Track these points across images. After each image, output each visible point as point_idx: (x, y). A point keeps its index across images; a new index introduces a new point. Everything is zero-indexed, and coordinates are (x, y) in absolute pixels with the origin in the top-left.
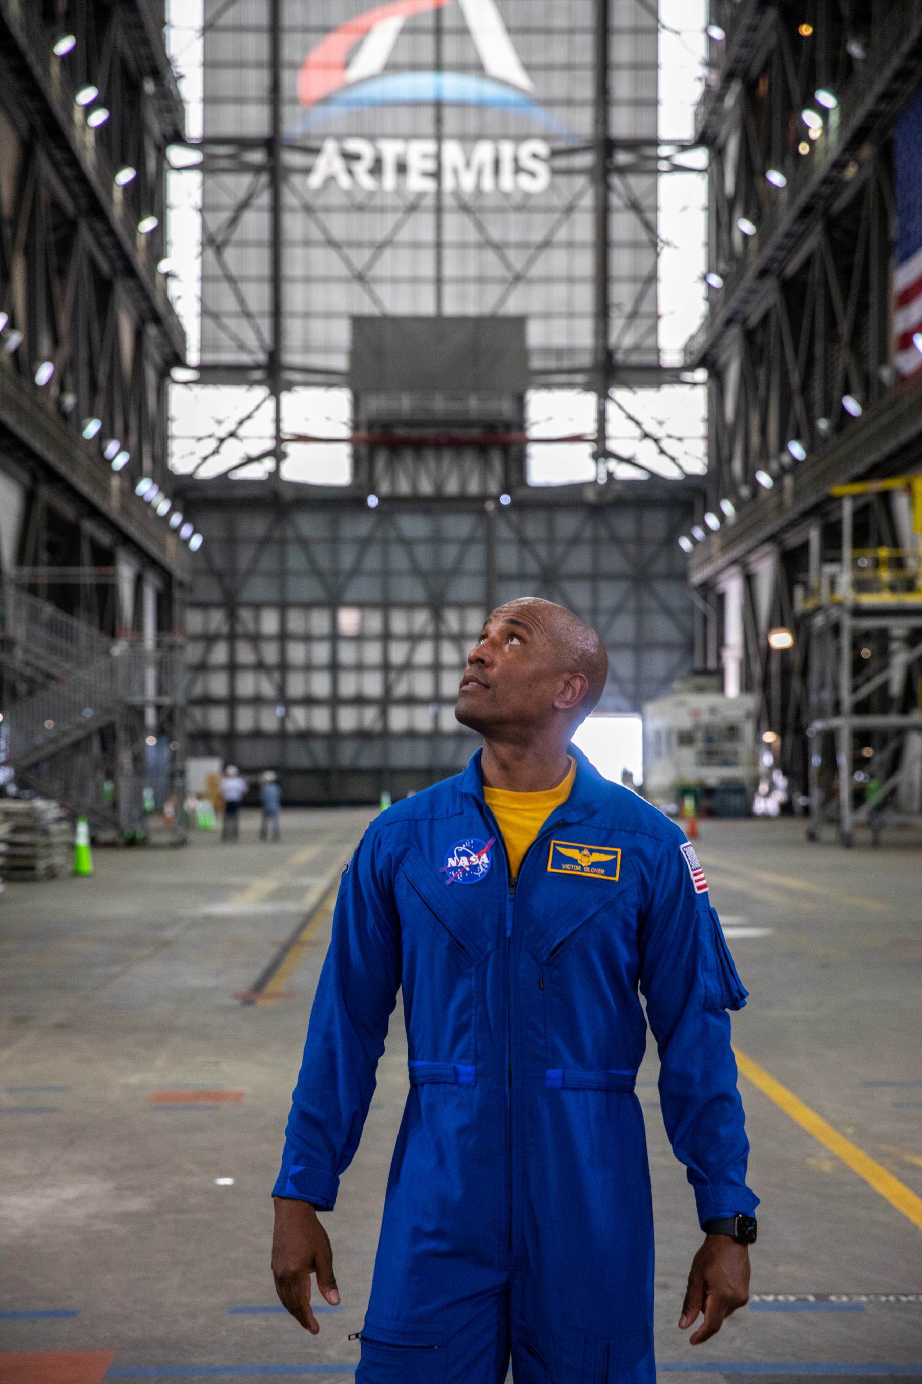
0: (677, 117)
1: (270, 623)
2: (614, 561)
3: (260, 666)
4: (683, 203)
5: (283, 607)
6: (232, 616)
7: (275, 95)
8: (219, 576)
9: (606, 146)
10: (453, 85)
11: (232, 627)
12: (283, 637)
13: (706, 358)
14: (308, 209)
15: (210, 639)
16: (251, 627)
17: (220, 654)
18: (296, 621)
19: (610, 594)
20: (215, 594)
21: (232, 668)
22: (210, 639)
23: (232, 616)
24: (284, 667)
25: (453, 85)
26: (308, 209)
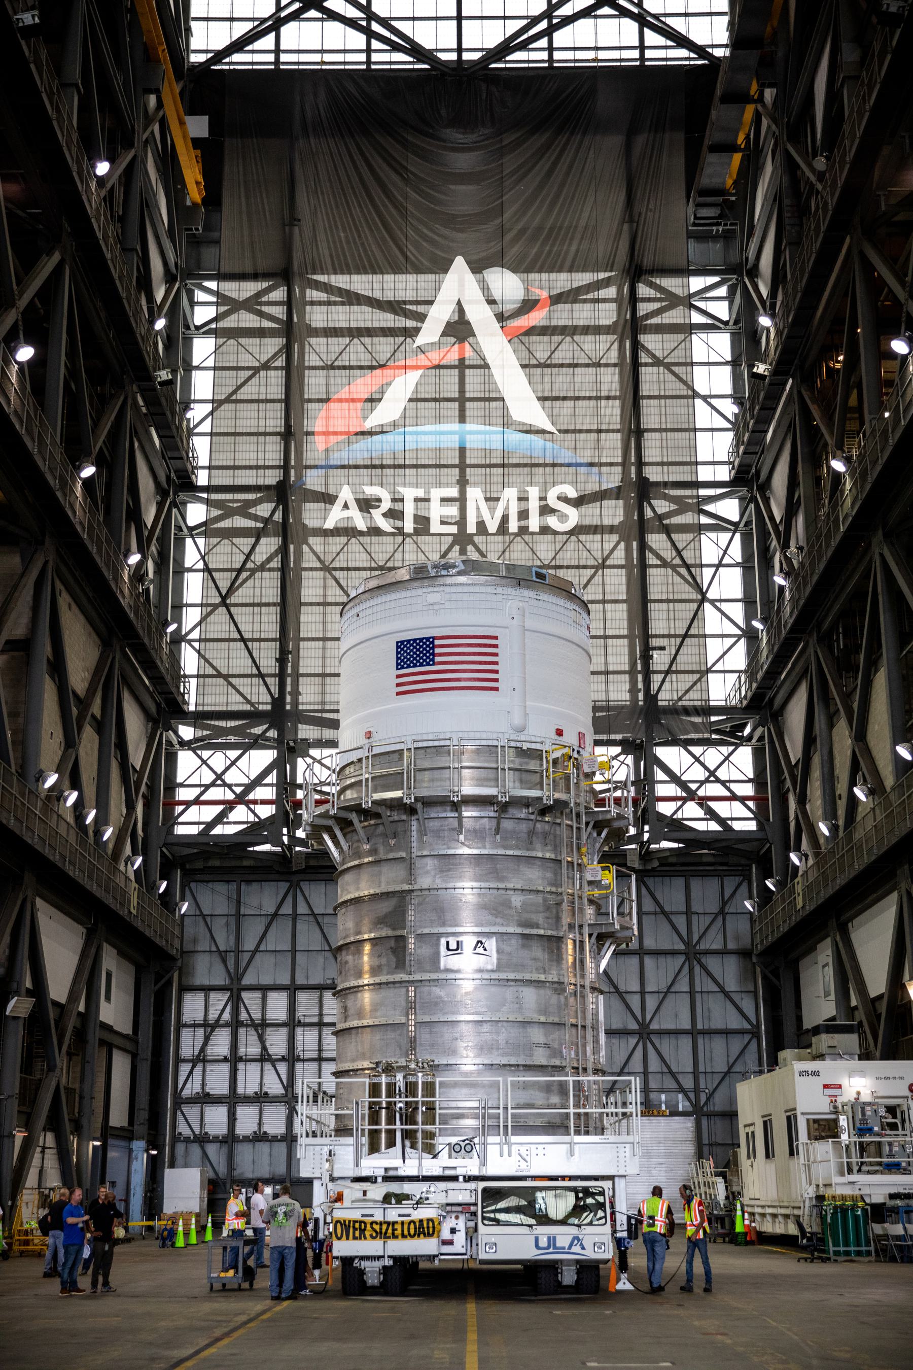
0: (715, 451)
1: (278, 1007)
2: (659, 937)
3: (264, 1058)
4: (721, 558)
5: (293, 989)
6: (236, 1001)
7: (290, 434)
8: (223, 956)
9: (642, 490)
10: (479, 435)
11: (236, 1013)
12: (292, 1023)
13: (762, 702)
14: (326, 569)
15: (209, 1027)
16: (257, 1016)
17: (220, 1044)
18: (306, 1004)
19: (658, 974)
20: (220, 978)
21: (234, 1060)
22: (209, 1027)
23: (236, 1001)
24: (292, 1058)
25: (479, 435)
26: (326, 569)
